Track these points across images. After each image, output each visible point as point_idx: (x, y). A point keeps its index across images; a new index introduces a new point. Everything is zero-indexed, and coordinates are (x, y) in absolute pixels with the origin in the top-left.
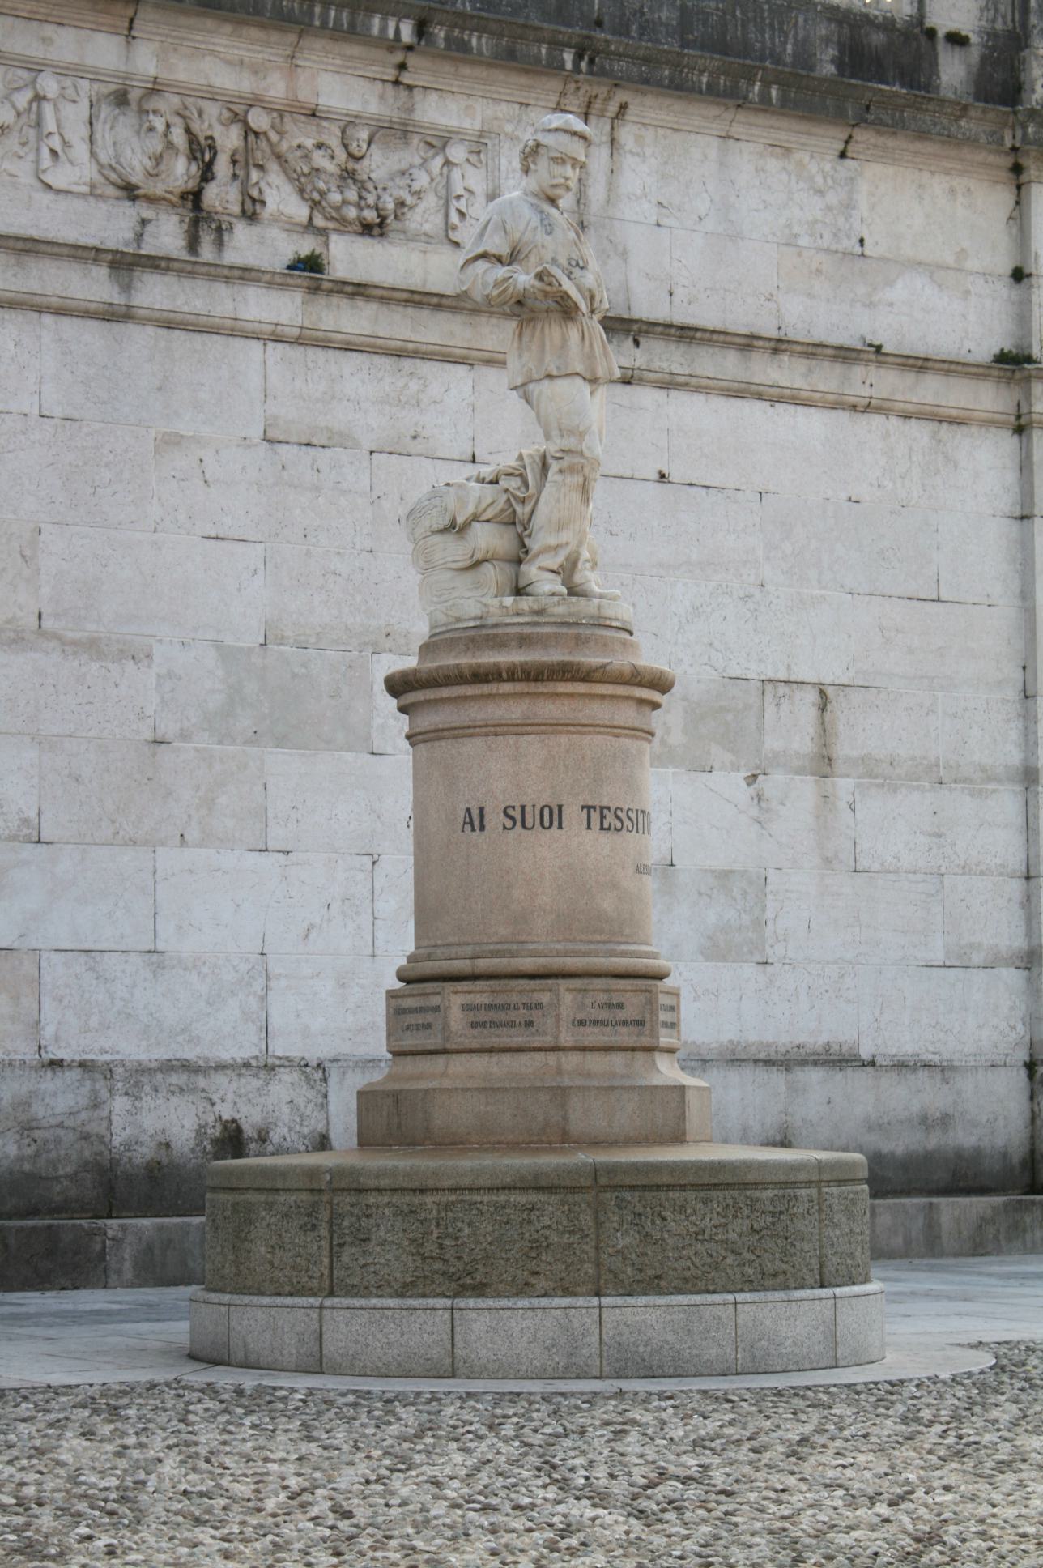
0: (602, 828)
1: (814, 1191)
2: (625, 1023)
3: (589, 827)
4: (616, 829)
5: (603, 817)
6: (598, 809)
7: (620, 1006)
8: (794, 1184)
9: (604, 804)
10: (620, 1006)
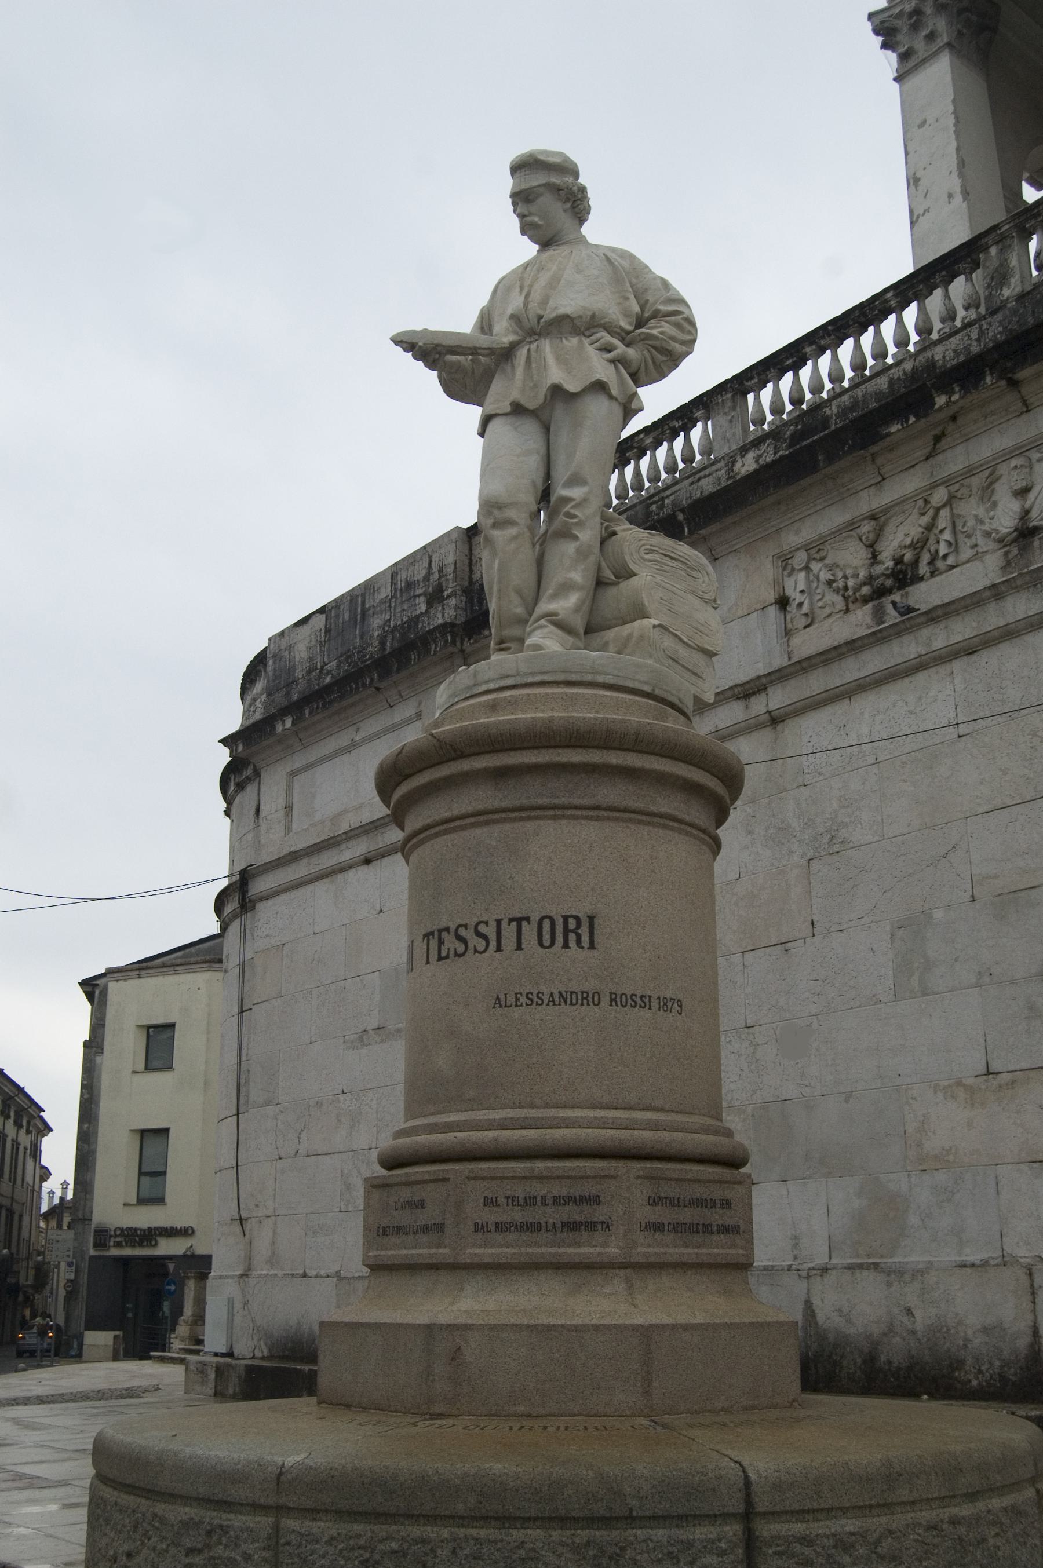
0: (440, 958)
1: (263, 1523)
2: (425, 1229)
3: (428, 962)
4: (456, 955)
5: (441, 942)
6: (436, 933)
7: (421, 1205)
8: (225, 1505)
9: (443, 925)
10: (421, 1205)
